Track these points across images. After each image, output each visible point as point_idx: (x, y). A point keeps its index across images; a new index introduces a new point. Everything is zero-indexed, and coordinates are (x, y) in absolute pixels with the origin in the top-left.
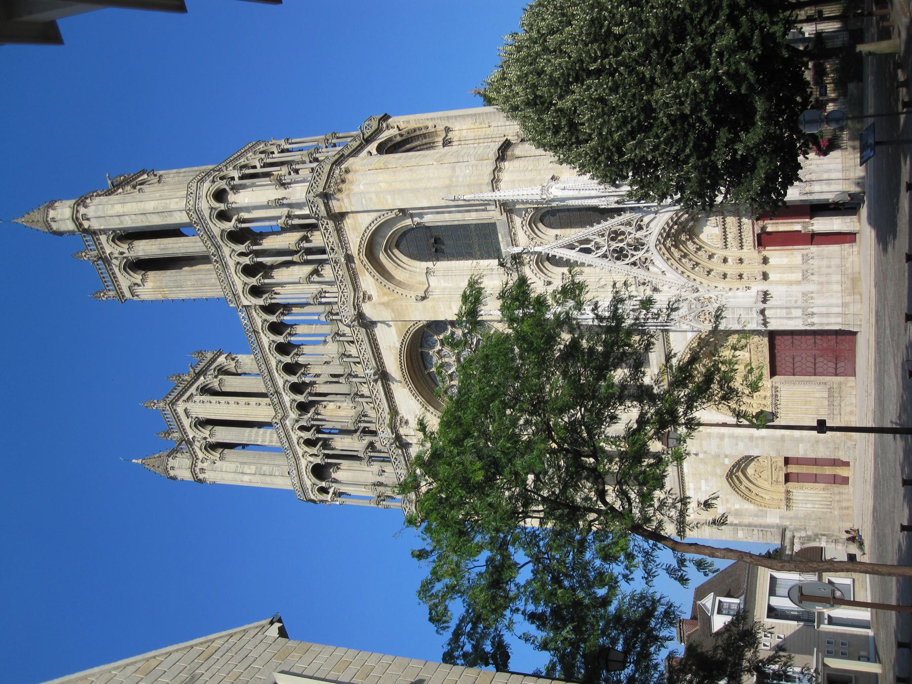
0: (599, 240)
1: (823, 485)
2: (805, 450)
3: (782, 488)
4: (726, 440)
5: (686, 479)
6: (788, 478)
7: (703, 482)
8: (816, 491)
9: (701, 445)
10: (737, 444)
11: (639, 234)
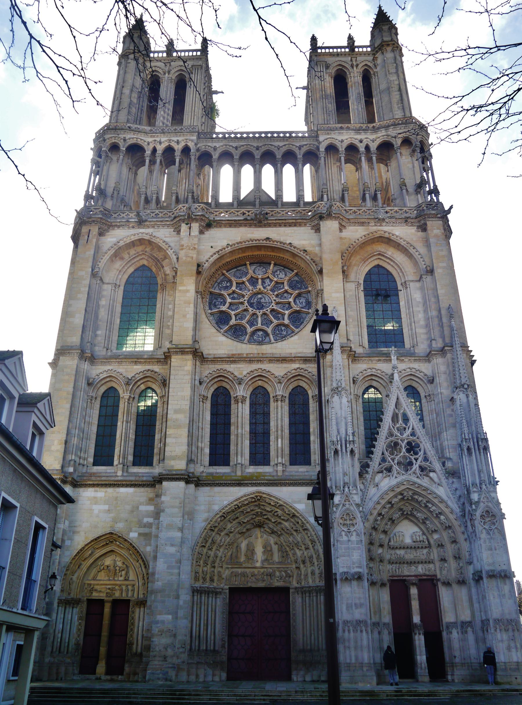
0: (408, 432)
1: (81, 642)
2: (163, 622)
3: (85, 596)
4: (179, 534)
5: (110, 490)
6: (95, 606)
7: (106, 507)
8: (76, 636)
9: (173, 507)
10: (172, 545)
11: (416, 467)
